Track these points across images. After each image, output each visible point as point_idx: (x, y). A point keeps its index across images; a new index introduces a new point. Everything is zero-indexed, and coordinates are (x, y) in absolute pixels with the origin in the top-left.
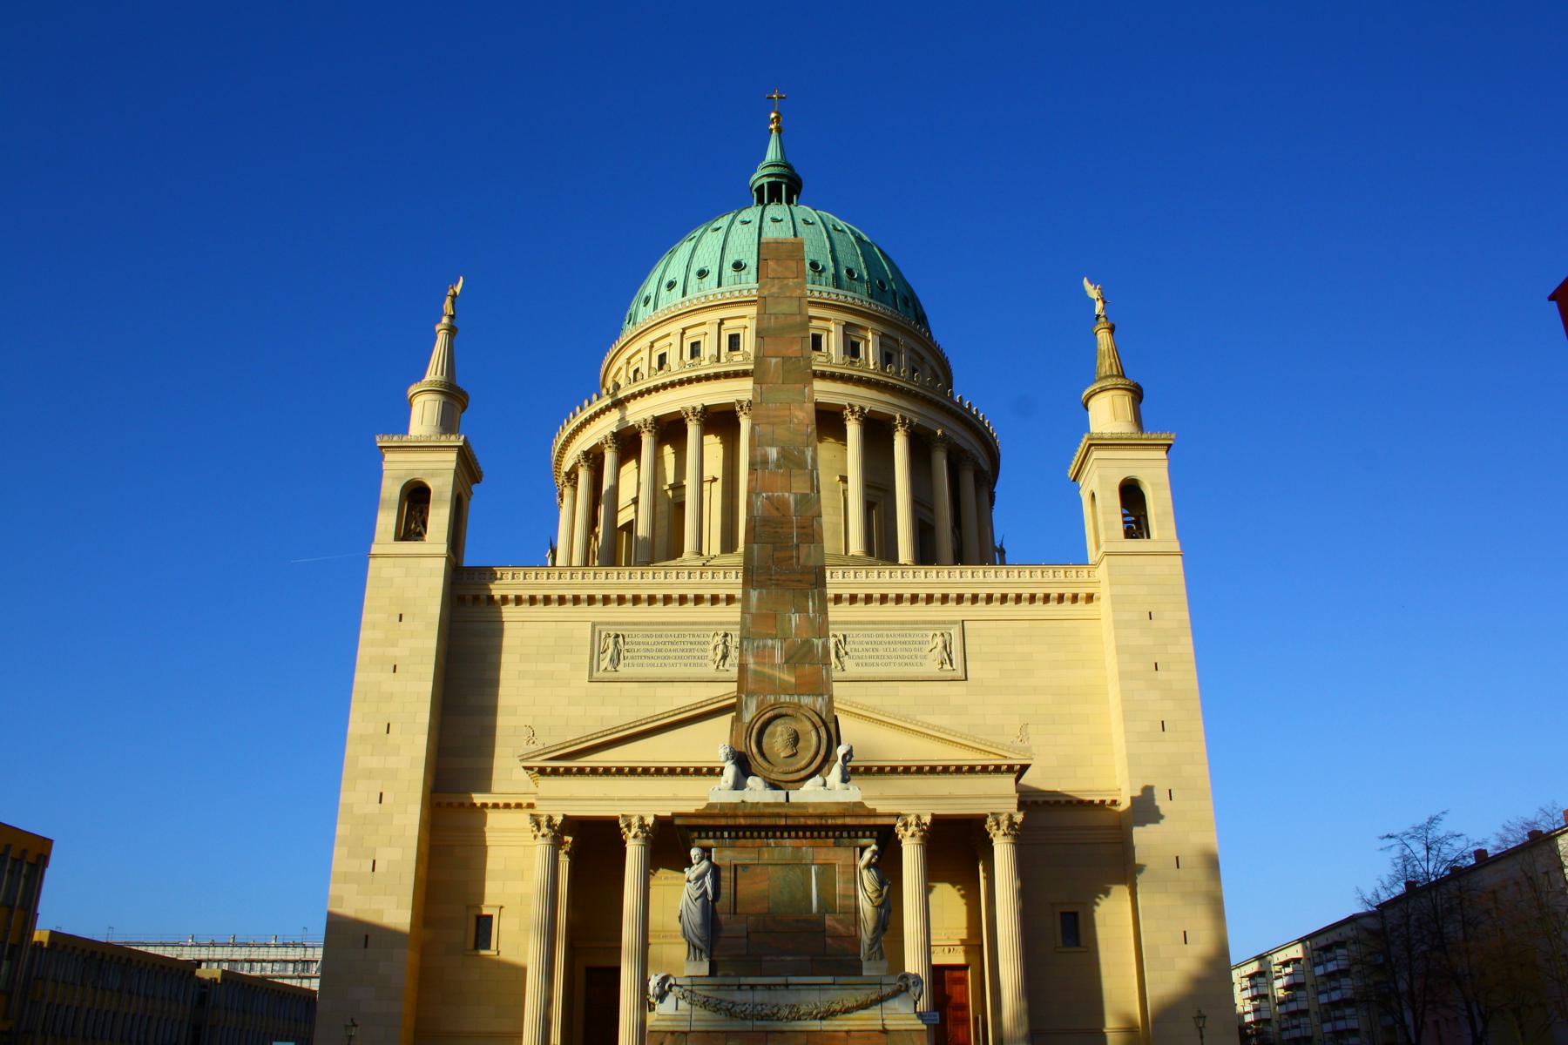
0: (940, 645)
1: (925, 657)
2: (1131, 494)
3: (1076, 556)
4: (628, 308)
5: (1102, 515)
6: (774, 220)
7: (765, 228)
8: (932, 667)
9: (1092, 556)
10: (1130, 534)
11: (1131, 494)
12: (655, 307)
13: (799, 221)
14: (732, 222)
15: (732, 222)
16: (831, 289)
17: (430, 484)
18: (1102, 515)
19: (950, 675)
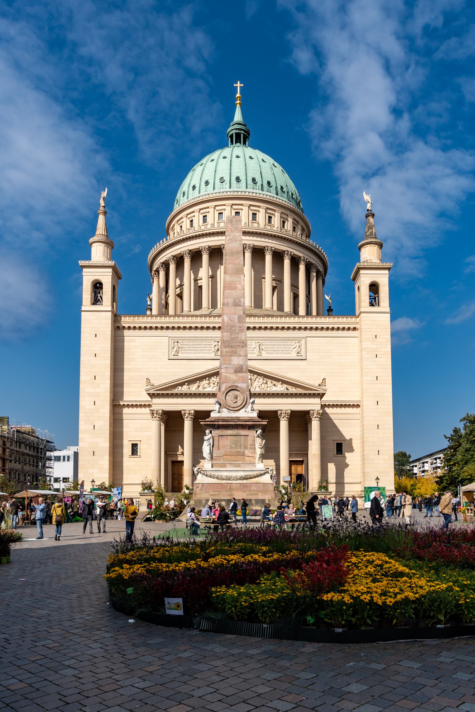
0: (298, 346)
1: (292, 351)
2: (374, 287)
3: (349, 310)
4: (176, 195)
5: (363, 295)
6: (238, 157)
7: (233, 162)
8: (293, 355)
9: (357, 313)
10: (372, 305)
11: (374, 287)
12: (188, 198)
13: (247, 157)
14: (219, 157)
15: (219, 157)
16: (261, 192)
17: (103, 281)
18: (363, 295)
19: (301, 358)
